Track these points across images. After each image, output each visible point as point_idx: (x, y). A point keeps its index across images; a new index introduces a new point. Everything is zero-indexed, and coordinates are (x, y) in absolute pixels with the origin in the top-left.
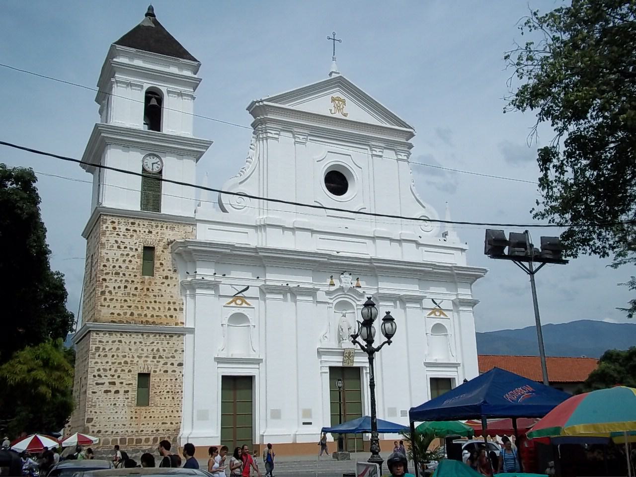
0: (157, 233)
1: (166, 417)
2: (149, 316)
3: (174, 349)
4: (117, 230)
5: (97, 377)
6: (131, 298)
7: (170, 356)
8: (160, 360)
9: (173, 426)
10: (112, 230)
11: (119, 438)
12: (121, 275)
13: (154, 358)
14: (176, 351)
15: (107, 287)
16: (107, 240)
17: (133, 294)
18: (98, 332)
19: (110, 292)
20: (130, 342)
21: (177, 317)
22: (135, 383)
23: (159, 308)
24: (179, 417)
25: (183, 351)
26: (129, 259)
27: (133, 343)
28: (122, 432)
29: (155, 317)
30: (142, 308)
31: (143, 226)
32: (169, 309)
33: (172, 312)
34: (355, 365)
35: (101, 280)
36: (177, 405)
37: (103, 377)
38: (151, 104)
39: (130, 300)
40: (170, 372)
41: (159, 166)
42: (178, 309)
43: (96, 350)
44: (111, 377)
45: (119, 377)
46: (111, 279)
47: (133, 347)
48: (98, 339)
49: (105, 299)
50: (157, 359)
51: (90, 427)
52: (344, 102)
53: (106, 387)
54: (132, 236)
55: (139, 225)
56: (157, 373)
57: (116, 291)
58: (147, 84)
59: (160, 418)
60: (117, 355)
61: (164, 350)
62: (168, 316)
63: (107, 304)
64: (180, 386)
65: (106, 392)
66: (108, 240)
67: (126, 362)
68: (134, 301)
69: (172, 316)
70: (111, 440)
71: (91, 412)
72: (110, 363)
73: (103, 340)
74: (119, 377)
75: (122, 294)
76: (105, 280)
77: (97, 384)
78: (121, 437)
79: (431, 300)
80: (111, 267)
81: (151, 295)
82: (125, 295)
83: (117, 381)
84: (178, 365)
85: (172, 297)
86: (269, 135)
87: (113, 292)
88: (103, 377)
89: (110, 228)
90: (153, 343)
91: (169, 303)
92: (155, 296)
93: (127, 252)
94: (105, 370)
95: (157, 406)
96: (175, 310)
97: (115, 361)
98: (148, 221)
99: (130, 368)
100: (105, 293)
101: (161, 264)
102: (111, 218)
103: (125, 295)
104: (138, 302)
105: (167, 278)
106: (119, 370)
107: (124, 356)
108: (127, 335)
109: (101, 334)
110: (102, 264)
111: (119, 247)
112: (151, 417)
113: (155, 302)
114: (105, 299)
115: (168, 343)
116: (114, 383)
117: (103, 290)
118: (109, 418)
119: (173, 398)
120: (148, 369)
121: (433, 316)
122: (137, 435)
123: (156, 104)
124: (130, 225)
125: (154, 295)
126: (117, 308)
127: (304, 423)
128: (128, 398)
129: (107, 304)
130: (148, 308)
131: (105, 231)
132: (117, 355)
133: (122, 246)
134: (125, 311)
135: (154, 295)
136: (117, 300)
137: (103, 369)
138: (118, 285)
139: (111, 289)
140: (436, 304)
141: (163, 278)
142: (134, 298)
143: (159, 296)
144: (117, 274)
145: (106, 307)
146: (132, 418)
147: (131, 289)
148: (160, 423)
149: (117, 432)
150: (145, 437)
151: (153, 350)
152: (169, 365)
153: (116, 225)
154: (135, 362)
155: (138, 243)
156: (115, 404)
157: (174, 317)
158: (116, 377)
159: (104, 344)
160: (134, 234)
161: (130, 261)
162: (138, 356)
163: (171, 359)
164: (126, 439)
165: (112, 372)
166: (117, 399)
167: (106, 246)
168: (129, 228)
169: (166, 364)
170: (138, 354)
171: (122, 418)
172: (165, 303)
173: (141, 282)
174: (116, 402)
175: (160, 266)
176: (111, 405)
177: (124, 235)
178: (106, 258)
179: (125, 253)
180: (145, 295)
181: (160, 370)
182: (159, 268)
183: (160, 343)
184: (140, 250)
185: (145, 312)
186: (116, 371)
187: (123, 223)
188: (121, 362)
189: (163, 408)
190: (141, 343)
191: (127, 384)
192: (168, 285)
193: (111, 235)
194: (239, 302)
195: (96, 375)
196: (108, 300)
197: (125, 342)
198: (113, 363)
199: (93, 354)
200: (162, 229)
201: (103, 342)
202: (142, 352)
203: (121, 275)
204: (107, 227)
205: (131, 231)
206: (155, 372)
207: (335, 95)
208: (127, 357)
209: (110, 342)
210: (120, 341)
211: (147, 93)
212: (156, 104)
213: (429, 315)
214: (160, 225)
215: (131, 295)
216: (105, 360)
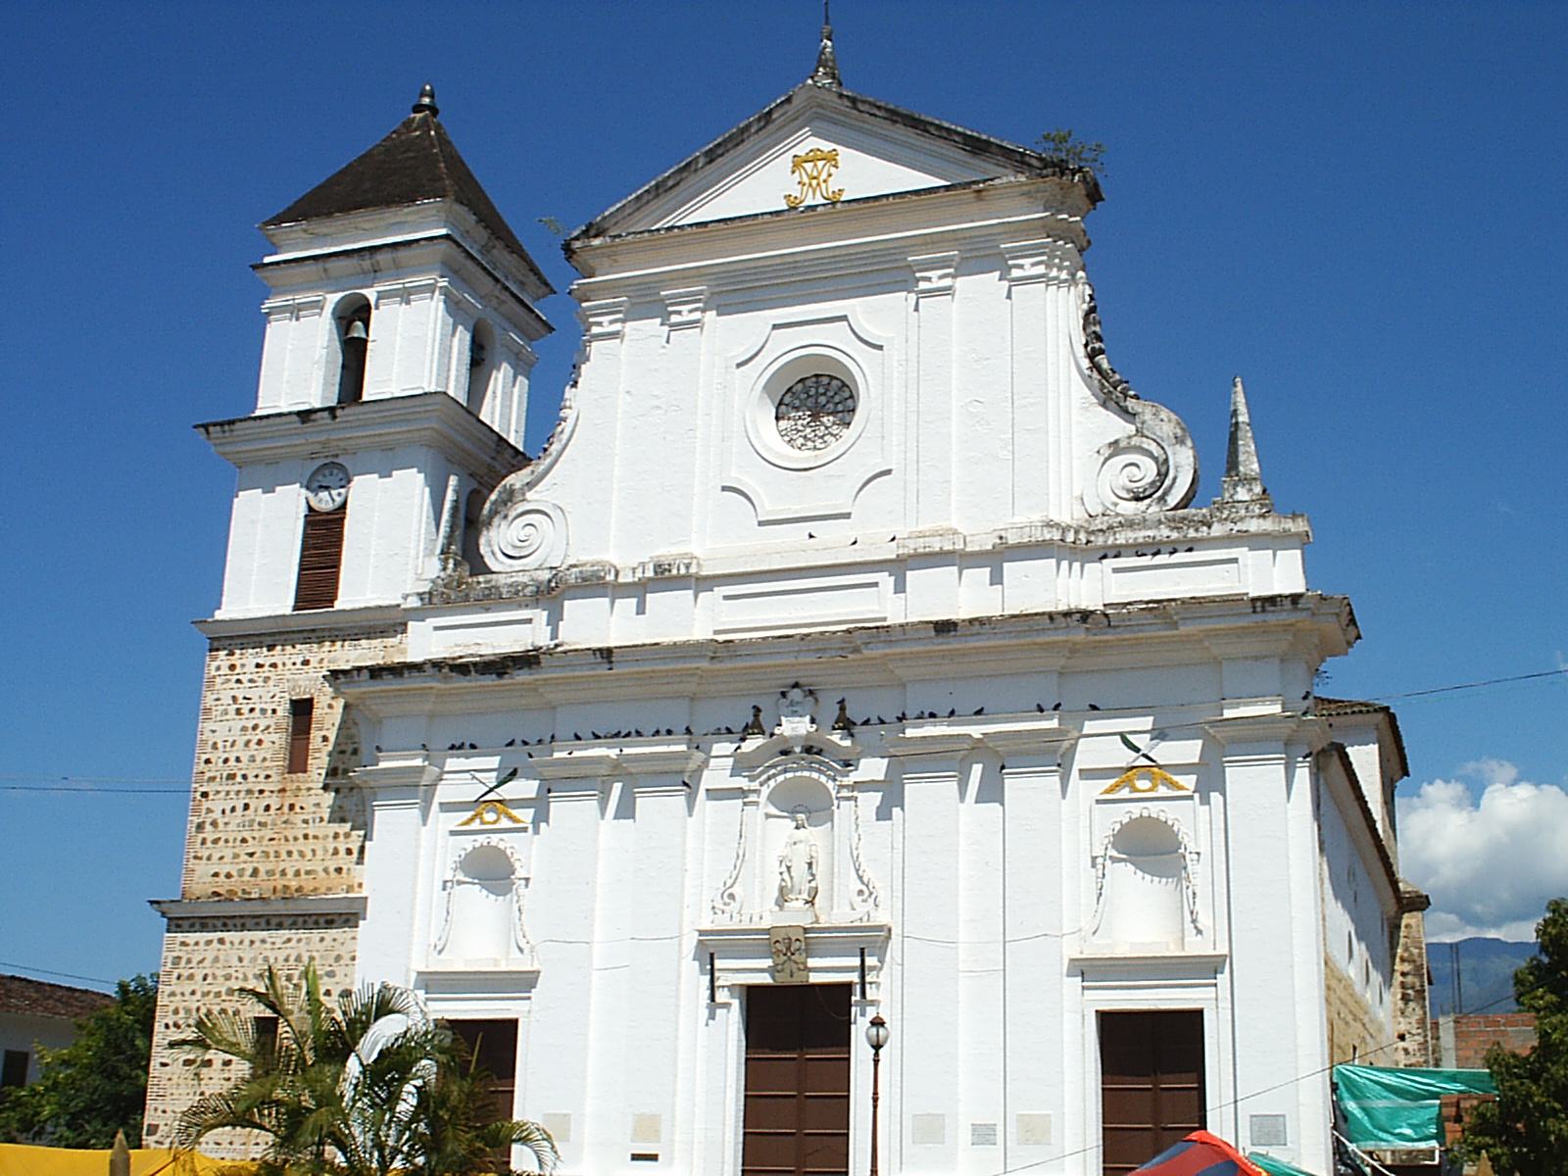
2: (290, 873)
3: (336, 953)
4: (237, 672)
5: (173, 1029)
6: (256, 834)
12: (239, 779)
14: (338, 958)
15: (209, 811)
17: (260, 824)
18: (180, 922)
19: (214, 824)
20: (241, 942)
25: (353, 958)
26: (258, 737)
33: (342, 860)
35: (199, 798)
39: (254, 838)
43: (173, 964)
46: (218, 792)
57: (226, 820)
62: (331, 870)
63: (205, 853)
69: (341, 869)
71: (156, 1109)
72: (198, 996)
75: (238, 825)
80: (221, 764)
81: (298, 819)
84: (341, 996)
87: (220, 822)
89: (225, 670)
92: (306, 822)
93: (255, 722)
97: (209, 988)
99: (238, 1005)
104: (271, 839)
107: (228, 977)
110: (204, 757)
111: (238, 712)
113: (306, 837)
114: (204, 842)
126: (225, 860)
127: (636, 1157)
129: (205, 853)
131: (214, 677)
133: (245, 710)
136: (227, 841)
137: (184, 1008)
139: (217, 815)
140: (1137, 750)
142: (262, 833)
143: (314, 822)
144: (231, 777)
145: (204, 861)
147: (256, 811)
151: (287, 960)
155: (279, 695)
157: (344, 871)
161: (260, 742)
167: (214, 713)
173: (279, 791)
177: (251, 681)
178: (210, 743)
179: (250, 725)
180: (285, 822)
182: (319, 750)
184: (283, 710)
185: (282, 865)
188: (220, 992)
193: (224, 686)
195: (171, 1024)
196: (209, 844)
197: (232, 943)
198: (206, 994)
199: (169, 973)
203: (239, 779)
207: (801, 150)
208: (233, 980)
215: (256, 827)
216: (188, 988)
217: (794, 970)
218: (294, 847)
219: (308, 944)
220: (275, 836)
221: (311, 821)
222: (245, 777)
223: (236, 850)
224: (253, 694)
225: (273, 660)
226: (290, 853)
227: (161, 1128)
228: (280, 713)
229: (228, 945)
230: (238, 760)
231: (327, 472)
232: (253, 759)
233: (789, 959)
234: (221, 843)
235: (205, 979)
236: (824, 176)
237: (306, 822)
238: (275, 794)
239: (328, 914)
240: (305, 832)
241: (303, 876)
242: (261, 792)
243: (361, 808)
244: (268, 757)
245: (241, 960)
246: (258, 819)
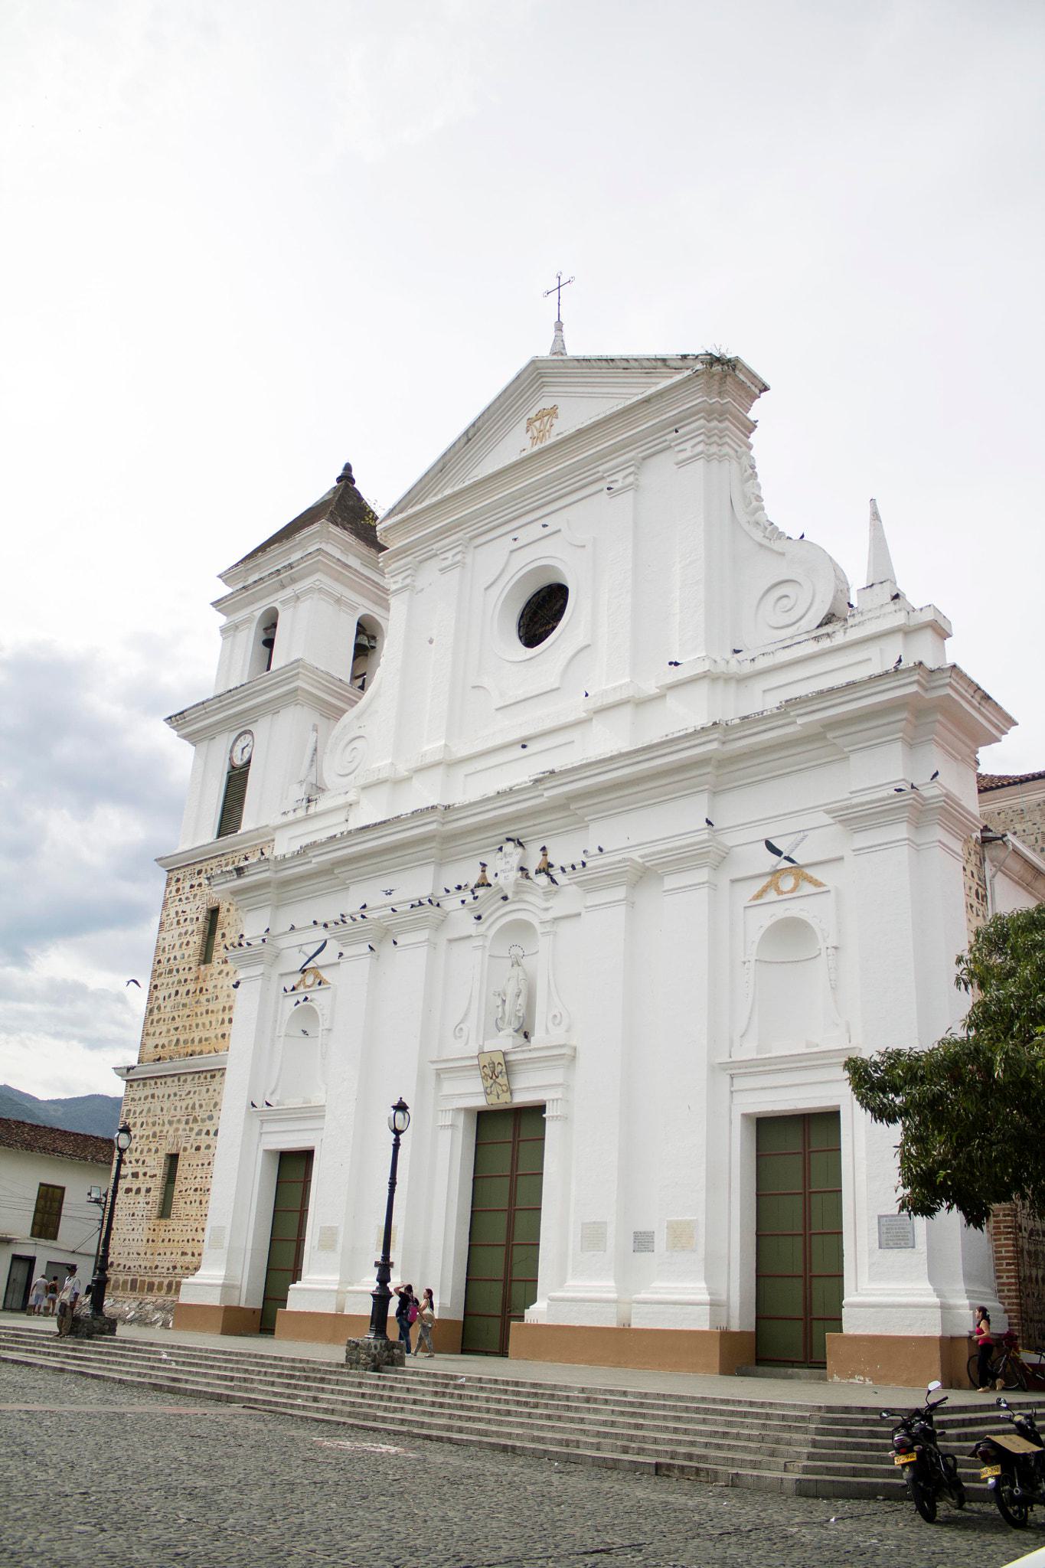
1: (188, 1241)
3: (213, 1102)
7: (205, 1117)
11: (130, 1278)
12: (175, 972)
13: (187, 1123)
15: (157, 998)
22: (160, 1172)
23: (211, 1022)
34: (522, 1098)
36: (204, 1217)
45: (144, 1162)
47: (166, 1106)
50: (191, 1125)
56: (187, 1153)
61: (201, 1106)
70: (156, 1283)
74: (144, 1162)
81: (203, 998)
89: (174, 893)
90: (190, 1092)
95: (179, 1218)
101: (223, 935)
104: (188, 1016)
107: (154, 1124)
110: (158, 959)
111: (178, 922)
112: (169, 1240)
115: (208, 1090)
119: (201, 1203)
121: (772, 896)
122: (150, 1274)
133: (182, 920)
140: (778, 853)
142: (184, 1012)
148: (180, 1253)
150: (132, 1277)
164: (137, 1280)
169: (199, 1133)
170: (170, 1118)
179: (183, 931)
180: (197, 1002)
185: (193, 1035)
186: (142, 1152)
189: (185, 1222)
196: (155, 1024)
197: (158, 1097)
203: (175, 972)
204: (171, 892)
206: (185, 1149)
207: (532, 414)
210: (153, 1096)
224: (187, 908)
226: (197, 1025)
228: (200, 920)
230: (175, 958)
231: (242, 738)
233: (495, 1082)
234: (161, 1022)
235: (142, 1126)
236: (548, 427)
239: (212, 1070)
245: (162, 1110)
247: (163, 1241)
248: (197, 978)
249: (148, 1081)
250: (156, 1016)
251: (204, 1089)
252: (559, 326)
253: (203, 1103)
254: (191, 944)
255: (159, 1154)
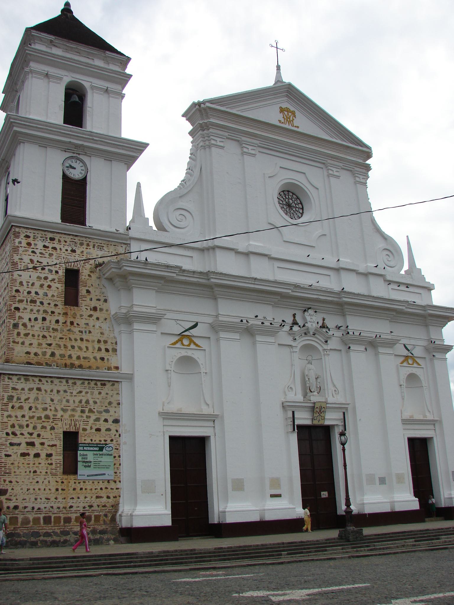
0: (82, 252)
1: (101, 489)
2: (74, 357)
3: (108, 401)
4: (31, 247)
5: (11, 436)
6: (51, 334)
8: (91, 414)
9: (110, 500)
10: (27, 246)
11: (42, 516)
12: (38, 303)
13: (83, 411)
14: (110, 403)
15: (20, 318)
16: (19, 259)
17: (53, 329)
18: (11, 377)
19: (25, 325)
20: (52, 391)
21: (110, 359)
22: (60, 444)
23: (87, 348)
24: (117, 489)
25: (119, 404)
27: (55, 391)
28: (45, 508)
29: (82, 360)
30: (65, 346)
31: (65, 244)
32: (100, 349)
33: (103, 354)
34: (327, 423)
35: (13, 310)
37: (19, 436)
38: (72, 100)
39: (51, 336)
40: (103, 430)
41: (83, 172)
42: (110, 350)
43: (8, 399)
44: (29, 436)
45: (39, 435)
46: (25, 309)
47: (56, 398)
48: (11, 385)
49: (19, 334)
51: (4, 501)
52: (293, 113)
53: (23, 448)
54: (51, 255)
55: (59, 241)
56: (87, 432)
58: (68, 78)
59: (94, 490)
60: (36, 407)
61: (95, 403)
62: (98, 358)
63: (21, 340)
64: (117, 449)
65: (23, 455)
66: (22, 259)
67: (47, 417)
68: (55, 337)
70: (31, 519)
71: (5, 481)
72: (27, 418)
73: (17, 387)
75: (40, 328)
76: (17, 309)
77: (12, 444)
78: (44, 515)
79: (403, 345)
81: (76, 330)
82: (43, 329)
83: (37, 442)
84: (113, 422)
85: (102, 333)
86: (213, 142)
87: (29, 325)
88: (19, 436)
89: (24, 244)
90: (81, 392)
91: (99, 341)
92: (81, 332)
94: (21, 426)
96: (107, 350)
97: (34, 414)
98: (71, 237)
99: (53, 424)
100: (18, 326)
101: (88, 292)
102: (24, 230)
103: (43, 329)
104: (60, 338)
105: (95, 309)
106: (39, 426)
107: (45, 409)
108: (47, 382)
109: (15, 378)
110: (15, 288)
112: (81, 489)
113: (82, 339)
114: (19, 334)
116: (32, 444)
117: (15, 322)
118: (28, 490)
120: (75, 425)
122: (65, 512)
123: (77, 99)
124: (49, 241)
125: (79, 331)
128: (51, 464)
129: (21, 340)
130: (73, 347)
132: (36, 407)
134: (44, 350)
135: (79, 331)
136: (33, 336)
137: (18, 425)
138: (35, 316)
139: (26, 320)
141: (91, 310)
142: (55, 334)
143: (86, 332)
144: (33, 302)
146: (57, 490)
147: (50, 322)
148: (94, 497)
149: (39, 509)
152: (102, 421)
153: (30, 240)
154: (59, 416)
156: (35, 472)
157: (106, 359)
158: (35, 435)
159: (19, 392)
160: (54, 253)
161: (49, 286)
162: (63, 410)
163: (104, 414)
164: (50, 517)
165: (30, 429)
166: (37, 465)
168: (47, 244)
169: (97, 420)
170: (62, 406)
171: (45, 489)
172: (93, 341)
174: (37, 469)
175: (86, 294)
176: (30, 472)
177: (41, 253)
178: (18, 281)
179: (43, 276)
180: (69, 330)
181: (91, 428)
182: (86, 297)
183: (90, 393)
184: (61, 273)
185: (69, 353)
187: (40, 238)
188: (41, 417)
190: (65, 391)
191: (49, 446)
192: (98, 319)
193: (25, 253)
194: (186, 342)
196: (22, 335)
197: (45, 390)
200: (88, 247)
201: (17, 389)
202: (68, 404)
203: (38, 303)
204: (20, 243)
205: (50, 249)
206: (85, 430)
207: (284, 106)
208: (49, 410)
209: (26, 389)
210: (39, 389)
211: (67, 89)
212: (77, 100)
213: (402, 363)
214: (85, 243)
216: (19, 413)
217: (320, 419)
218: (73, 343)
219: (92, 393)
220: (63, 337)
221: (84, 332)
222: (42, 303)
223: (40, 341)
225: (54, 246)
227: (10, 491)
229: (43, 392)
232: (46, 295)
233: (320, 415)
234: (30, 336)
237: (81, 332)
238: (61, 315)
240: (81, 337)
241: (82, 360)
242: (53, 312)
243: (111, 329)
244: (55, 294)
246: (52, 327)
247: (74, 489)
248: (66, 314)
249: (31, 378)
250: (21, 328)
251: (96, 392)
252: (278, 68)
253: (98, 401)
254: (53, 288)
255: (56, 430)
